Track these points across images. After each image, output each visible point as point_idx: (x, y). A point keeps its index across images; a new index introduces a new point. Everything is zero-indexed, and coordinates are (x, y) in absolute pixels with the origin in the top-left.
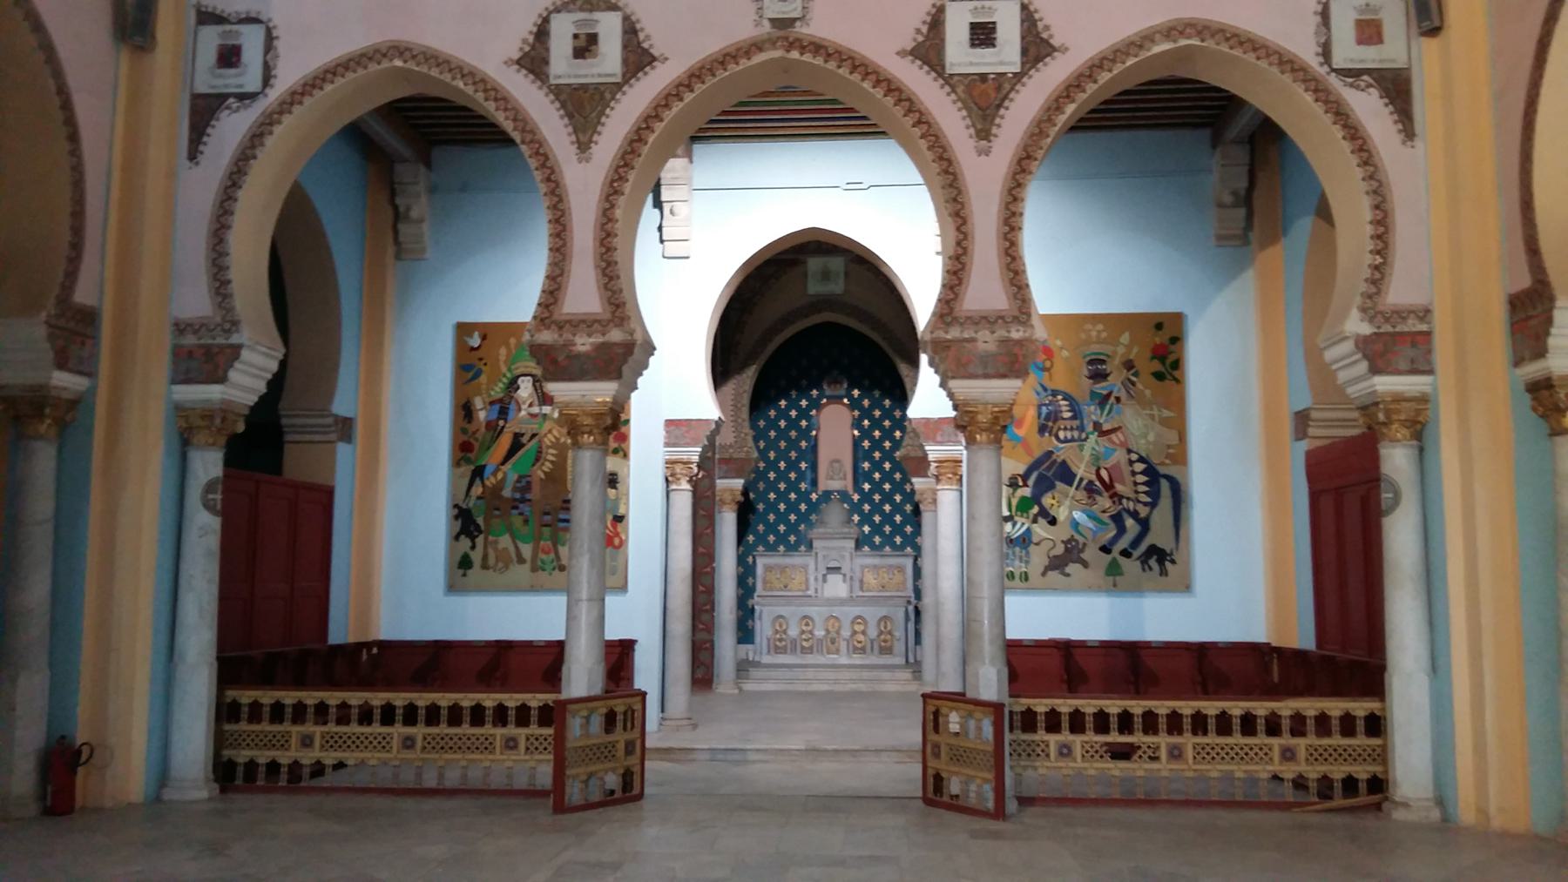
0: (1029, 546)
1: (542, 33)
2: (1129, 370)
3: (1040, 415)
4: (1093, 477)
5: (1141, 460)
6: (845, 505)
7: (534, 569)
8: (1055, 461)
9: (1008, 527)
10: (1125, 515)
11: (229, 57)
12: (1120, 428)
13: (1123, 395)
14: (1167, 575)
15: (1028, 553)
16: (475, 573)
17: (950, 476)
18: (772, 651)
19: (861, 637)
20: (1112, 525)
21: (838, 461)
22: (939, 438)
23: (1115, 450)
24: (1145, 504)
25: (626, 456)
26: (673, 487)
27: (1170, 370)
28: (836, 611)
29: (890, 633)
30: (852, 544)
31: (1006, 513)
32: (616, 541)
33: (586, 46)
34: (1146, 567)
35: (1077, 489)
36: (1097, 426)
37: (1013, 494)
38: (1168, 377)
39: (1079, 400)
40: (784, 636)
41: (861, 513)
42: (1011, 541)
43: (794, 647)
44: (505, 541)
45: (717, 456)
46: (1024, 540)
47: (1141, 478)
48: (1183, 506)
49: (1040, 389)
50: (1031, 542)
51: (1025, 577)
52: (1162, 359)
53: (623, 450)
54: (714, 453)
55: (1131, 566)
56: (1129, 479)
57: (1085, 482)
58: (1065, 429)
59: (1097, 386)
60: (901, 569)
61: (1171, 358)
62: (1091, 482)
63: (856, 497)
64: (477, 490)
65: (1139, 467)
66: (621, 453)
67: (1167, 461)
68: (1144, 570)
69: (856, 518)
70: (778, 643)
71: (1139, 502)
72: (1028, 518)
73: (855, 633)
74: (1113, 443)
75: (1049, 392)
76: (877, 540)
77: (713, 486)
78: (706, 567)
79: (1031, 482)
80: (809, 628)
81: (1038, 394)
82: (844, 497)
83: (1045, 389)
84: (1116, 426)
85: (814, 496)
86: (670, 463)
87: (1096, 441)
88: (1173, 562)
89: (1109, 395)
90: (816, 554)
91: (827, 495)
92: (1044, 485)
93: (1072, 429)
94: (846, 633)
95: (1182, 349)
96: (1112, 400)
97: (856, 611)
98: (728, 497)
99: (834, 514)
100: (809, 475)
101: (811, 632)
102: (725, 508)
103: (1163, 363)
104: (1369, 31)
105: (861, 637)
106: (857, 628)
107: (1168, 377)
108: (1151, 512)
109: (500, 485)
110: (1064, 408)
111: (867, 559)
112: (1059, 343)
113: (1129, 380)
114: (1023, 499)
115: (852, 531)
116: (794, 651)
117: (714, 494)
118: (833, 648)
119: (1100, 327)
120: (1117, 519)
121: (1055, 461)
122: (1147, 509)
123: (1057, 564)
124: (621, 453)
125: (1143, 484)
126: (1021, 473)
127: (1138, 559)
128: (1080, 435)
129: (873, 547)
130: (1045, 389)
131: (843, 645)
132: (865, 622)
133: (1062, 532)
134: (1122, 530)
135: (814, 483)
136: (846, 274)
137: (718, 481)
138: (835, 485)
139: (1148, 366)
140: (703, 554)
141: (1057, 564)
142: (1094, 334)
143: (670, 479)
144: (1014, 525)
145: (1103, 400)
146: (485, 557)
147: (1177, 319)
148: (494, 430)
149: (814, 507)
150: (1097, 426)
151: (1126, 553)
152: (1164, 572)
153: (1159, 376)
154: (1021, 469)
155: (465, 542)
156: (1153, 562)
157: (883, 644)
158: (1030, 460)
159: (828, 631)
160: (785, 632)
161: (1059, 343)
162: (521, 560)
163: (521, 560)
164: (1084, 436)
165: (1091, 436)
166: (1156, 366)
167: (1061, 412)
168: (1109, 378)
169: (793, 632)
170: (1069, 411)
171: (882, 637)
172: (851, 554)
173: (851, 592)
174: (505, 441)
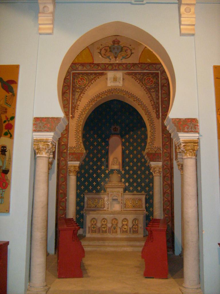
6: (119, 175)
17: (192, 151)
18: (90, 232)
19: (126, 227)
21: (116, 158)
22: (186, 130)
25: (11, 136)
26: (38, 155)
28: (116, 216)
29: (137, 225)
30: (121, 190)
32: (4, 184)
40: (95, 226)
41: (125, 178)
43: (99, 230)
45: (68, 152)
53: (10, 133)
54: (67, 151)
60: (140, 200)
63: (123, 172)
66: (9, 135)
69: (123, 180)
70: (93, 229)
73: (123, 225)
76: (131, 188)
77: (66, 164)
78: (63, 199)
80: (105, 223)
82: (119, 172)
85: (107, 172)
86: (36, 142)
90: (108, 193)
91: (112, 171)
94: (120, 225)
97: (123, 217)
98: (72, 169)
99: (115, 178)
100: (105, 163)
101: (106, 225)
102: (71, 174)
105: (126, 227)
106: (124, 223)
111: (128, 196)
115: (122, 185)
116: (99, 232)
117: (67, 167)
118: (115, 231)
124: (9, 135)
129: (130, 191)
131: (119, 230)
132: (127, 220)
135: (107, 166)
136: (123, 79)
137: (69, 162)
138: (116, 167)
140: (61, 193)
143: (37, 151)
149: (107, 176)
157: (134, 229)
159: (113, 225)
160: (95, 224)
169: (99, 225)
171: (134, 226)
172: (122, 194)
173: (122, 208)
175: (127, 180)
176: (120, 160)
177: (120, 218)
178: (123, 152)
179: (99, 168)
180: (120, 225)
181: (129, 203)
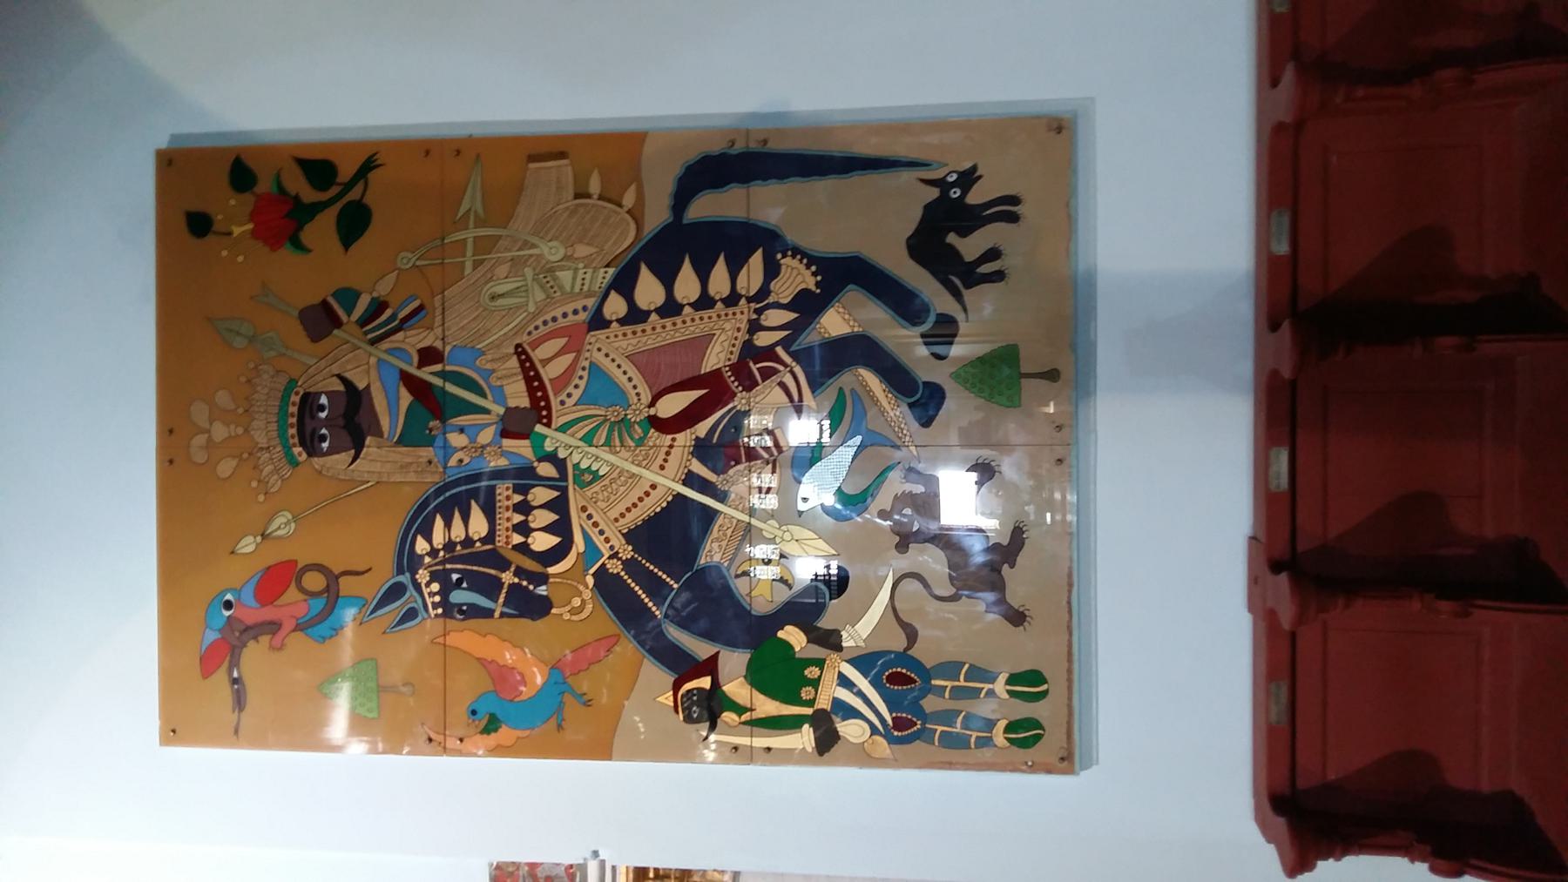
0: (916, 665)
2: (337, 323)
3: (474, 612)
4: (684, 439)
5: (624, 283)
8: (628, 564)
9: (851, 730)
10: (810, 338)
12: (520, 351)
13: (414, 340)
14: (1014, 200)
15: (950, 669)
20: (846, 379)
23: (594, 369)
24: (772, 271)
27: (334, 191)
31: (805, 738)
34: (985, 268)
35: (721, 497)
36: (514, 426)
37: (740, 709)
38: (354, 195)
39: (433, 478)
42: (899, 724)
46: (896, 679)
47: (687, 285)
48: (775, 146)
49: (396, 608)
50: (904, 657)
51: (1028, 681)
52: (301, 213)
56: (690, 325)
57: (698, 467)
58: (524, 529)
59: (385, 423)
61: (298, 185)
62: (702, 449)
65: (649, 291)
67: (629, 199)
68: (999, 276)
71: (764, 292)
72: (820, 663)
74: (570, 372)
75: (405, 579)
79: (701, 649)
81: (411, 614)
83: (395, 592)
84: (514, 362)
87: (563, 429)
88: (968, 178)
89: (408, 380)
93: (524, 508)
95: (269, 151)
96: (427, 374)
103: (315, 209)
107: (354, 195)
108: (797, 252)
110: (458, 532)
112: (248, 545)
113: (364, 321)
114: (757, 678)
119: (200, 412)
121: (628, 564)
122: (788, 263)
125: (704, 278)
126: (669, 678)
127: (957, 295)
128: (546, 482)
130: (395, 592)
142: (220, 432)
144: (850, 713)
150: (514, 426)
152: (1007, 209)
153: (354, 224)
154: (656, 681)
156: (970, 247)
158: (627, 647)
161: (248, 545)
164: (546, 469)
165: (549, 446)
166: (321, 231)
167: (468, 542)
168: (361, 386)
170: (466, 519)
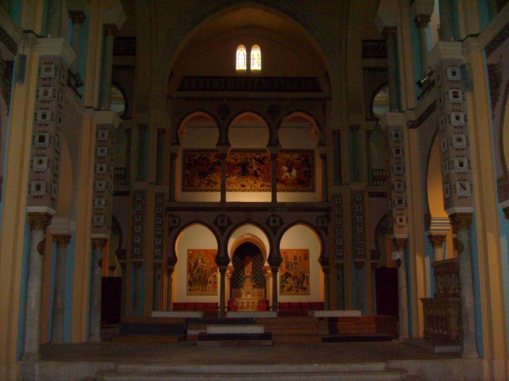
1: (216, 220)
7: (202, 291)
11: (174, 221)
16: (192, 292)
33: (223, 221)
44: (197, 286)
55: (300, 290)
64: (192, 278)
82: (250, 277)
91: (247, 276)
92: (287, 277)
94: (251, 305)
99: (248, 280)
104: (323, 223)
109: (196, 277)
111: (255, 290)
120: (299, 284)
123: (288, 290)
131: (250, 308)
133: (289, 285)
134: (299, 284)
135: (244, 274)
138: (249, 274)
139: (303, 258)
141: (288, 290)
145: (296, 263)
146: (193, 289)
147: (308, 250)
148: (195, 267)
149: (244, 279)
151: (299, 288)
153: (305, 259)
155: (190, 287)
162: (200, 290)
163: (200, 290)
174: (196, 269)
175: (255, 282)
176: (251, 270)
177: (251, 301)
178: (253, 266)
179: (239, 275)
180: (251, 305)
181: (256, 294)
